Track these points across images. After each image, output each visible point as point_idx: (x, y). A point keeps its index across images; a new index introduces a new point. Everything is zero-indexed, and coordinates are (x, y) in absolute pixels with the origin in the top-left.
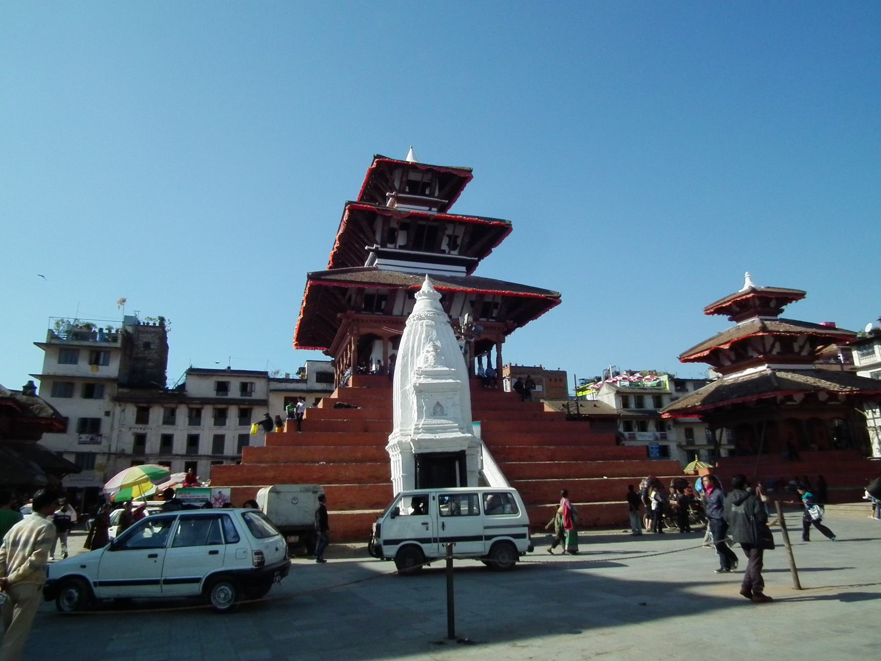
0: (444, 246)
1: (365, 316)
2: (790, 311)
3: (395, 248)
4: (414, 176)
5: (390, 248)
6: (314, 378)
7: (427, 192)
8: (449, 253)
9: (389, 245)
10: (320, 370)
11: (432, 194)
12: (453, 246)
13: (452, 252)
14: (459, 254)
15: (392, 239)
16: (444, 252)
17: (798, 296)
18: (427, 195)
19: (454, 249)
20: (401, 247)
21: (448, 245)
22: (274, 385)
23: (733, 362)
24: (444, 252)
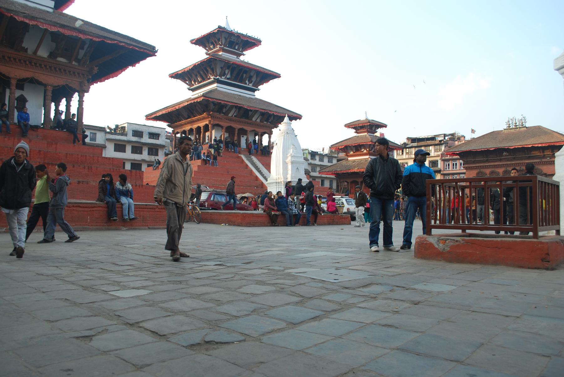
0: (247, 82)
1: (217, 114)
2: (379, 131)
4: (233, 39)
5: (223, 79)
6: (130, 134)
7: (236, 48)
10: (134, 129)
11: (238, 49)
12: (250, 82)
13: (251, 85)
14: (253, 86)
15: (224, 74)
16: (246, 84)
17: (385, 126)
18: (236, 50)
20: (228, 79)
23: (354, 152)
24: (246, 84)
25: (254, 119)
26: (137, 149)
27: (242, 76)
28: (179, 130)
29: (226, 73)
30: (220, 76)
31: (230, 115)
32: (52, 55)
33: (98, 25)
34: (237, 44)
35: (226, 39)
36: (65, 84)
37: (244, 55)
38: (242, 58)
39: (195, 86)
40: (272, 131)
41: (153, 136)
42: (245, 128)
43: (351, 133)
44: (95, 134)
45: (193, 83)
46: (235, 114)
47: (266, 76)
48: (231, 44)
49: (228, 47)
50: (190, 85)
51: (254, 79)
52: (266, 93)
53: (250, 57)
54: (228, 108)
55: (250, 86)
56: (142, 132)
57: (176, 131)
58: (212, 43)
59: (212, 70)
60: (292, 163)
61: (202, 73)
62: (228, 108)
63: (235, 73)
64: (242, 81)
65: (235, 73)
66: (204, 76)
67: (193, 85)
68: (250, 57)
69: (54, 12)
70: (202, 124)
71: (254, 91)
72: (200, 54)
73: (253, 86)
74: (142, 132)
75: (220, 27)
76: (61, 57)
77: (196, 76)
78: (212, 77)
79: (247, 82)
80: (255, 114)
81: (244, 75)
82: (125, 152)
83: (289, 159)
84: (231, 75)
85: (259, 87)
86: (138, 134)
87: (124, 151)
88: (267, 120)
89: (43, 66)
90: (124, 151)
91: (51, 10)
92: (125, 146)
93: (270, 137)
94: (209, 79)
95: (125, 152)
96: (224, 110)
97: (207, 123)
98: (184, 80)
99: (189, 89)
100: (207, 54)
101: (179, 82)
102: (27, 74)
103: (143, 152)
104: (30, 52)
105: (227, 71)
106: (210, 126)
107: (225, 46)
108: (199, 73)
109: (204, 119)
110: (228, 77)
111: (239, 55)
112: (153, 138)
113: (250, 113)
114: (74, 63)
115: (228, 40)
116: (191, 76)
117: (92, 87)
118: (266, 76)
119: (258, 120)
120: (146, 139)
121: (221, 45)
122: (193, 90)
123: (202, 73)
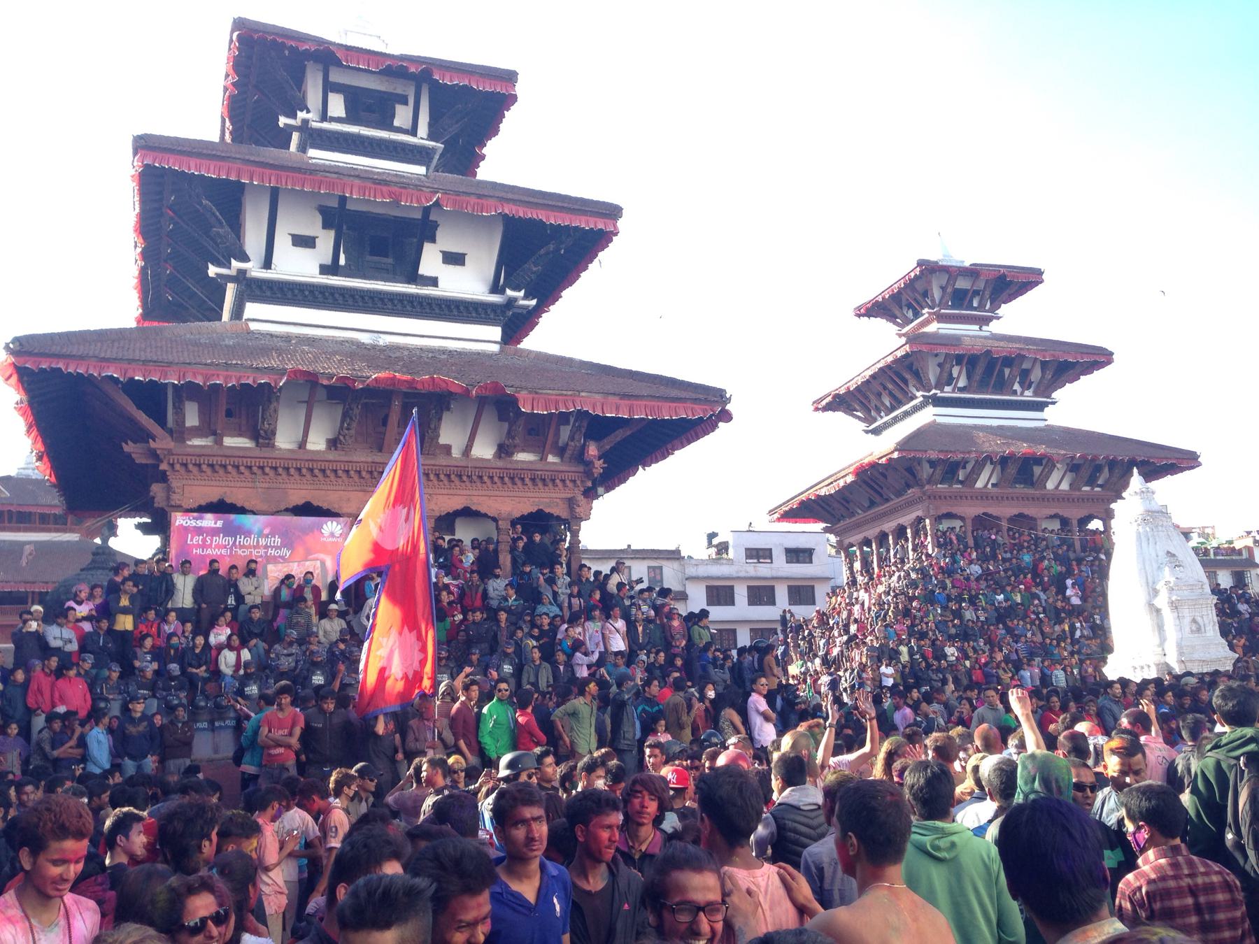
0: (1016, 387)
3: (953, 391)
4: (962, 284)
5: (948, 392)
7: (975, 304)
8: (1022, 394)
9: (947, 389)
11: (981, 307)
12: (1026, 384)
13: (1027, 393)
14: (1036, 394)
15: (950, 380)
16: (1015, 393)
18: (975, 309)
19: (1028, 388)
20: (962, 390)
21: (1021, 384)
22: (691, 571)
24: (1015, 393)
25: (1050, 485)
26: (761, 594)
27: (1001, 373)
28: (852, 540)
29: (955, 374)
30: (939, 386)
31: (979, 484)
32: (504, 450)
33: (595, 361)
34: (976, 293)
35: (943, 289)
36: (534, 509)
37: (998, 318)
38: (995, 327)
39: (879, 422)
41: (798, 557)
42: (1026, 511)
44: (661, 568)
45: (873, 413)
46: (993, 480)
47: (1072, 362)
48: (960, 299)
49: (953, 307)
50: (869, 420)
51: (1036, 375)
52: (1077, 407)
53: (1017, 320)
54: (969, 467)
55: (1028, 396)
56: (770, 550)
57: (847, 542)
58: (910, 306)
59: (917, 375)
60: (1175, 606)
61: (890, 386)
62: (969, 467)
63: (979, 370)
64: (1002, 386)
65: (979, 370)
66: (899, 395)
67: (875, 420)
68: (1017, 320)
69: (502, 350)
71: (1040, 407)
72: (884, 342)
73: (1036, 394)
74: (770, 550)
75: (921, 263)
76: (523, 451)
77: (879, 395)
78: (919, 394)
80: (1050, 472)
81: (1007, 371)
82: (733, 603)
83: (1162, 601)
84: (969, 377)
85: (1054, 395)
86: (759, 554)
87: (730, 601)
88: (1091, 482)
89: (485, 478)
90: (730, 601)
91: (495, 348)
92: (731, 589)
94: (913, 398)
95: (733, 603)
96: (961, 475)
97: (920, 513)
98: (849, 410)
99: (867, 432)
100: (900, 336)
101: (840, 416)
102: (456, 503)
104: (456, 453)
105: (955, 371)
107: (942, 305)
108: (885, 388)
109: (910, 504)
110: (961, 384)
111: (986, 321)
112: (798, 562)
113: (1037, 470)
114: (551, 458)
115: (949, 290)
116: (867, 398)
117: (596, 504)
118: (1072, 362)
119: (1065, 486)
120: (780, 566)
121: (930, 307)
122: (877, 432)
123: (890, 386)
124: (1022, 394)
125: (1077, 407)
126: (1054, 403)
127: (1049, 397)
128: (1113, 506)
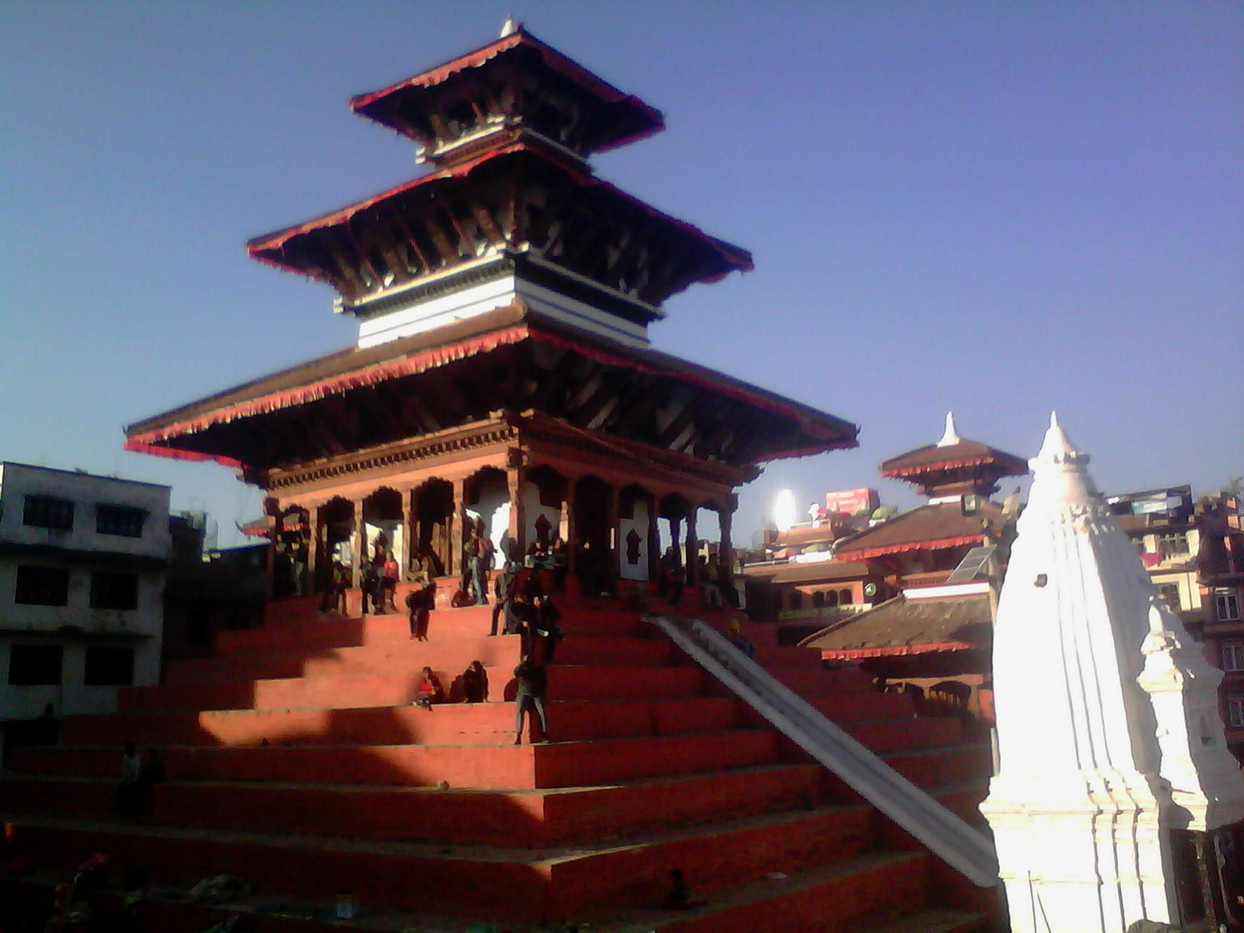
10: (34, 491)
16: (616, 287)
20: (556, 260)
40: (736, 496)
43: (904, 497)
52: (693, 329)
55: (632, 297)
70: (456, 469)
71: (644, 318)
79: (622, 283)
93: (725, 525)
103: (72, 597)
106: (513, 476)
112: (116, 532)
119: (689, 450)
120: (85, 536)
124: (626, 292)
125: (693, 329)
126: (660, 317)
127: (657, 303)
128: (735, 490)
